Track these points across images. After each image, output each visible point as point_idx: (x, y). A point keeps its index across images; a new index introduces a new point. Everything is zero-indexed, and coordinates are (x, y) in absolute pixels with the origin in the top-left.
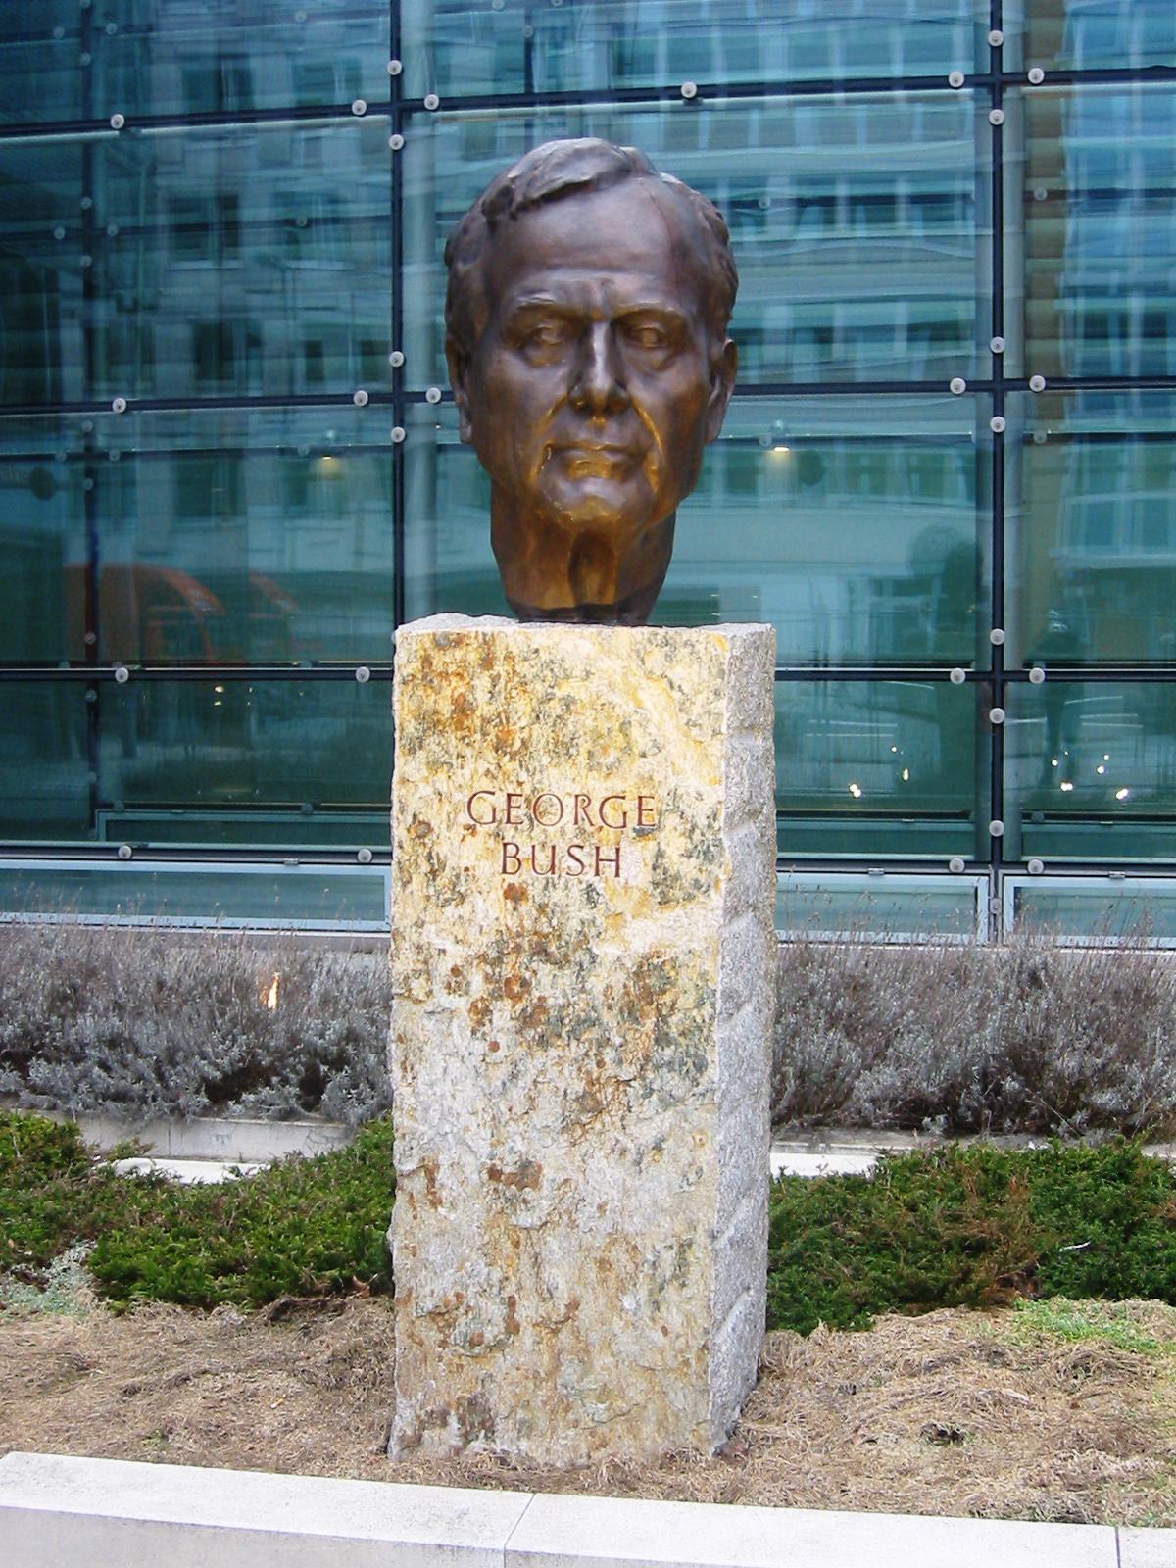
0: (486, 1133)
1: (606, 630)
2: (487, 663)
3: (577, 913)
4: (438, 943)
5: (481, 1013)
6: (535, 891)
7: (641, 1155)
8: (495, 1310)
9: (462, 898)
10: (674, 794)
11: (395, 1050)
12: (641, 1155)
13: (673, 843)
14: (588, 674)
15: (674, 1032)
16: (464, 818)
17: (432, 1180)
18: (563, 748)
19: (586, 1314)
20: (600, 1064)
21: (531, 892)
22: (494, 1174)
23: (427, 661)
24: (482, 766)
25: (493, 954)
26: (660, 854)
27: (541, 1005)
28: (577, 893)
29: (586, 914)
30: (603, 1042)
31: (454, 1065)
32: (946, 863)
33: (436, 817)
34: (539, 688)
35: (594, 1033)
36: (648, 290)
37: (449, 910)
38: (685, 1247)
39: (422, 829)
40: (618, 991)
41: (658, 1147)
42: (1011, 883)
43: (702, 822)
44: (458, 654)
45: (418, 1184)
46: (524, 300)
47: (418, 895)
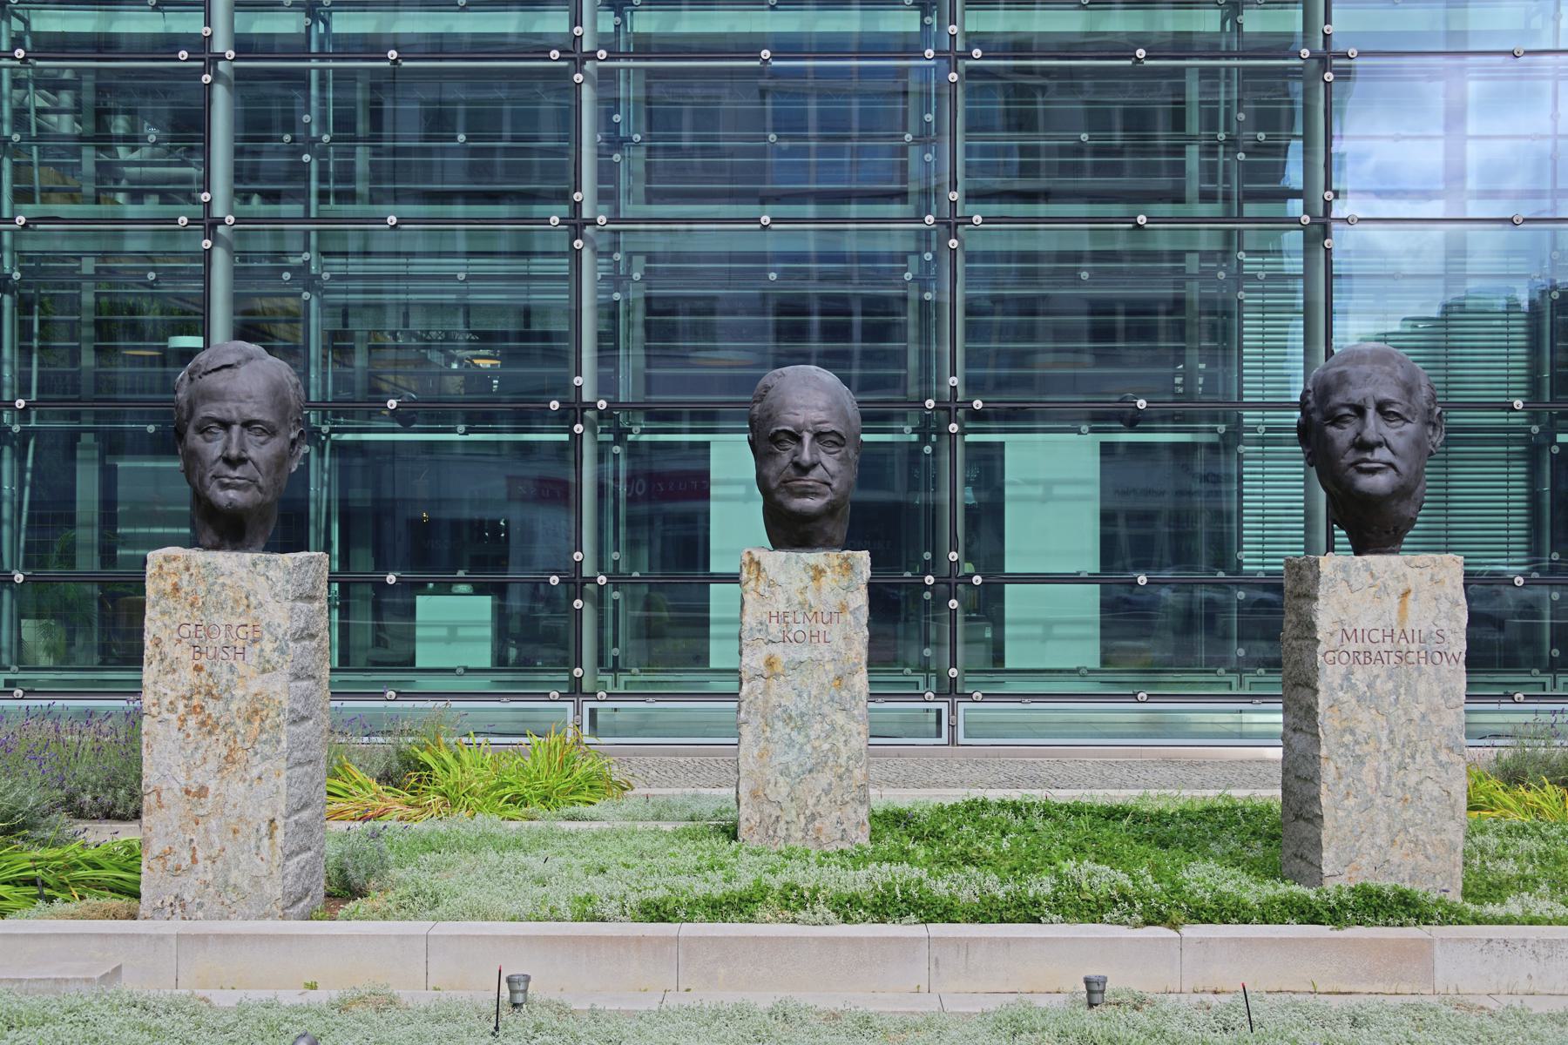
0: (184, 774)
1: (240, 554)
2: (188, 569)
3: (226, 676)
4: (164, 691)
5: (183, 721)
6: (207, 668)
7: (252, 781)
8: (186, 854)
9: (174, 671)
10: (268, 625)
11: (145, 739)
12: (252, 781)
13: (268, 646)
14: (232, 573)
15: (267, 727)
16: (176, 636)
17: (159, 796)
18: (220, 606)
19: (229, 852)
20: (235, 742)
21: (206, 668)
22: (188, 792)
23: (161, 567)
24: (184, 613)
25: (188, 695)
26: (262, 650)
27: (209, 716)
28: (225, 668)
29: (229, 677)
31: (170, 744)
33: (164, 635)
34: (211, 580)
35: (233, 729)
36: (259, 411)
37: (169, 676)
39: (158, 643)
40: (243, 710)
41: (260, 778)
43: (280, 636)
44: (174, 564)
45: (153, 797)
46: (204, 414)
47: (155, 670)
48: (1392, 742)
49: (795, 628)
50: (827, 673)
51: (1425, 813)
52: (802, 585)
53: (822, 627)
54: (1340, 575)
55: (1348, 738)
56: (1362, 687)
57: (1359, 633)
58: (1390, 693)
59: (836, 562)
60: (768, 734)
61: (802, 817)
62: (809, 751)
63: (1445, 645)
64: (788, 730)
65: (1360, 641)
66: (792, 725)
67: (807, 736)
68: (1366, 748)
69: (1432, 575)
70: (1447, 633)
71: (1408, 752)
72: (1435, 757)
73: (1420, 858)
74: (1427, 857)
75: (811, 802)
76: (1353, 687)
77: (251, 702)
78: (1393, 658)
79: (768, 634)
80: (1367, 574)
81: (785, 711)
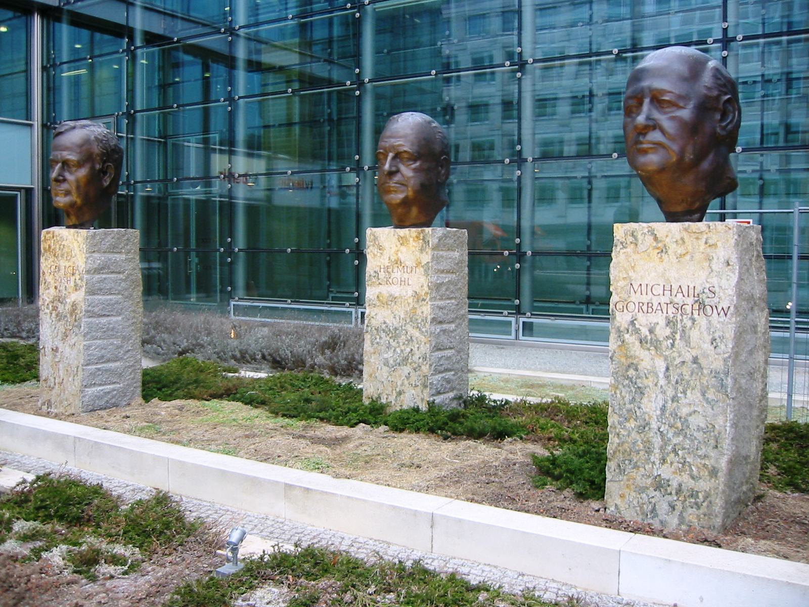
27: (59, 313)
30: (67, 321)
32: (502, 313)
38: (78, 367)
42: (522, 320)
48: (667, 377)
49: (393, 275)
50: (409, 304)
51: (692, 441)
52: (396, 249)
53: (406, 276)
54: (630, 239)
55: (631, 372)
56: (645, 331)
57: (644, 287)
58: (668, 338)
59: (414, 235)
60: (378, 340)
61: (394, 392)
62: (399, 352)
63: (716, 300)
64: (388, 338)
65: (644, 292)
66: (390, 335)
67: (398, 343)
68: (645, 381)
69: (707, 239)
70: (717, 289)
71: (680, 388)
72: (703, 395)
73: (685, 478)
74: (693, 478)
75: (399, 383)
76: (637, 331)
77: (72, 306)
78: (671, 310)
79: (379, 279)
80: (652, 238)
81: (387, 327)
